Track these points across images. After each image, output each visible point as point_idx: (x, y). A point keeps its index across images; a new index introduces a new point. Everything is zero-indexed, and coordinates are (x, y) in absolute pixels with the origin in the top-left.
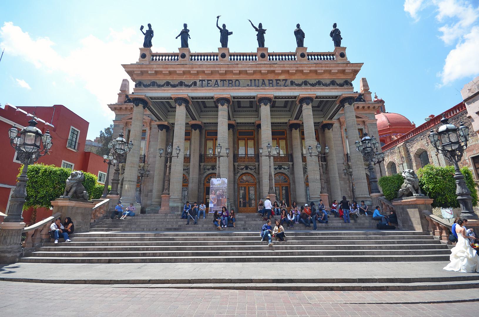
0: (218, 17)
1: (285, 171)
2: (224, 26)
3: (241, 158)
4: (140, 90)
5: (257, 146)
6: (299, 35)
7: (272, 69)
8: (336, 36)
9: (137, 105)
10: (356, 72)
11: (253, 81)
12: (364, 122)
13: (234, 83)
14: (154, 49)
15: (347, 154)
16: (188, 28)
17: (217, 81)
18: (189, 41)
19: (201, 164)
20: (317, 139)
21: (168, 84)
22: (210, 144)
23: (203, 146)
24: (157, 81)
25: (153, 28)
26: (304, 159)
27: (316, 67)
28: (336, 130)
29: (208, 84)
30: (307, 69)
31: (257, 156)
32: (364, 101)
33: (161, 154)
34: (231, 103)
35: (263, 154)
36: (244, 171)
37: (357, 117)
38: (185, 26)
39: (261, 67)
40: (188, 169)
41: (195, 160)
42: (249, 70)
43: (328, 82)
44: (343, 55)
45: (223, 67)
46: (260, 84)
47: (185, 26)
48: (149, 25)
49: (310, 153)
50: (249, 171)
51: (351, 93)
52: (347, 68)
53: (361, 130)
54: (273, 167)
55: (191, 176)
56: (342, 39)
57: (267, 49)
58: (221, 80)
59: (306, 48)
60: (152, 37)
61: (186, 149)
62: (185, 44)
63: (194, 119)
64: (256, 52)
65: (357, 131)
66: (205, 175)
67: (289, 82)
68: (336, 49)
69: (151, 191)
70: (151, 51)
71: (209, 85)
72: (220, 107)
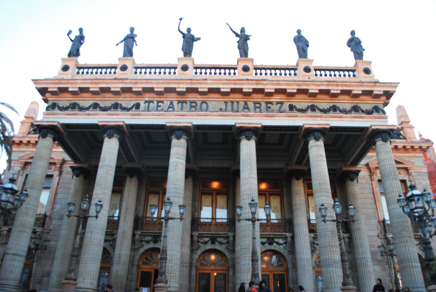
0: (181, 19)
1: (281, 249)
2: (189, 30)
3: (205, 224)
4: (53, 114)
5: (232, 206)
6: (300, 44)
8: (355, 45)
9: (44, 136)
10: (388, 95)
11: (229, 104)
12: (406, 169)
13: (198, 107)
14: (82, 60)
15: (384, 221)
16: (135, 33)
17: (172, 103)
18: (135, 50)
19: (136, 232)
20: (334, 195)
21: (95, 106)
22: (153, 200)
23: (142, 203)
25: (85, 33)
26: (312, 229)
27: (328, 85)
28: (364, 181)
29: (158, 106)
31: (232, 221)
32: (405, 138)
33: (70, 212)
34: (193, 135)
35: (242, 217)
36: (209, 246)
37: (397, 162)
38: (132, 30)
39: (242, 84)
40: (114, 240)
41: (126, 227)
42: (224, 88)
43: (348, 107)
44: (367, 71)
45: (183, 83)
46: (241, 108)
47: (132, 30)
48: (81, 30)
49: (324, 216)
50: (217, 246)
51: (385, 124)
53: (403, 182)
54: (258, 240)
55: (117, 252)
56: (364, 50)
57: (252, 60)
58: (179, 102)
59: (312, 61)
60: (81, 44)
61: (113, 207)
62: (128, 52)
63: (130, 159)
64: (236, 64)
65: (399, 183)
66: (142, 250)
67: (286, 106)
68: (356, 63)
69: (48, 274)
70: (77, 61)
71: (159, 108)
72: (174, 141)
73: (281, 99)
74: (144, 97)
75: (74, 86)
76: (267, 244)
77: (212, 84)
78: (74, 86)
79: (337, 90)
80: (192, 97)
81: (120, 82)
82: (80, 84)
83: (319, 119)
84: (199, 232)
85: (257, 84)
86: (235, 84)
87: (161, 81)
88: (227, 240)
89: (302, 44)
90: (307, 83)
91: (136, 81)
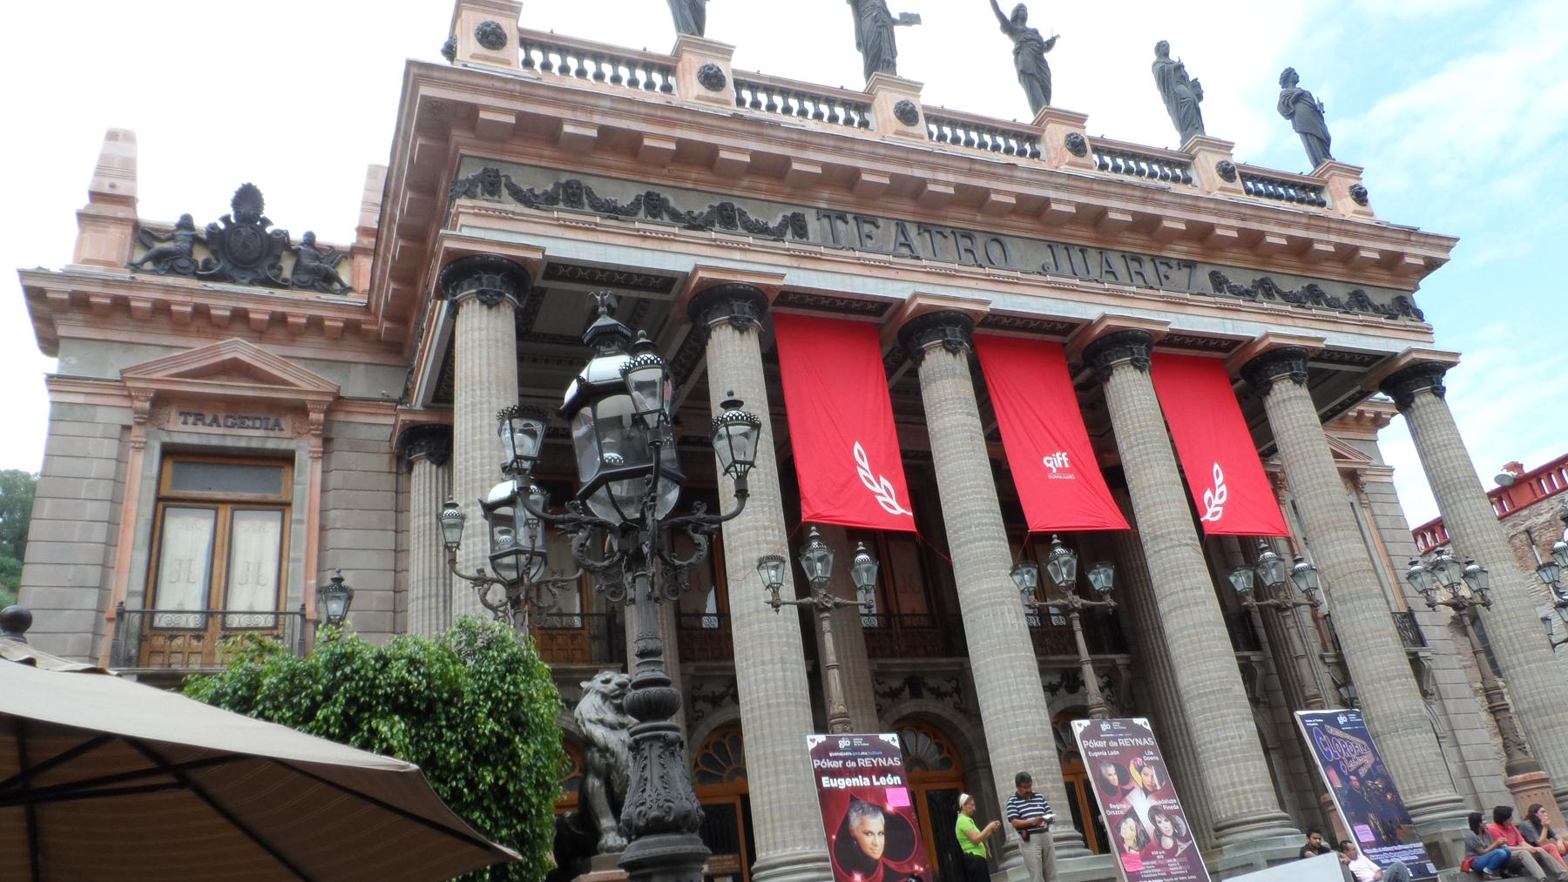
7: (1150, 210)
24: (593, 184)
27: (1308, 227)
30: (1277, 229)
39: (1106, 195)
51: (1428, 347)
52: (1407, 249)
67: (1202, 276)
73: (1188, 253)
74: (814, 199)
75: (581, 116)
76: (1062, 691)
77: (1028, 183)
78: (581, 116)
79: (1328, 243)
80: (959, 218)
81: (749, 133)
82: (604, 113)
83: (1289, 321)
84: (881, 661)
85: (1144, 200)
86: (1089, 192)
87: (882, 151)
88: (954, 684)
89: (1179, 90)
90: (1262, 213)
91: (803, 138)
